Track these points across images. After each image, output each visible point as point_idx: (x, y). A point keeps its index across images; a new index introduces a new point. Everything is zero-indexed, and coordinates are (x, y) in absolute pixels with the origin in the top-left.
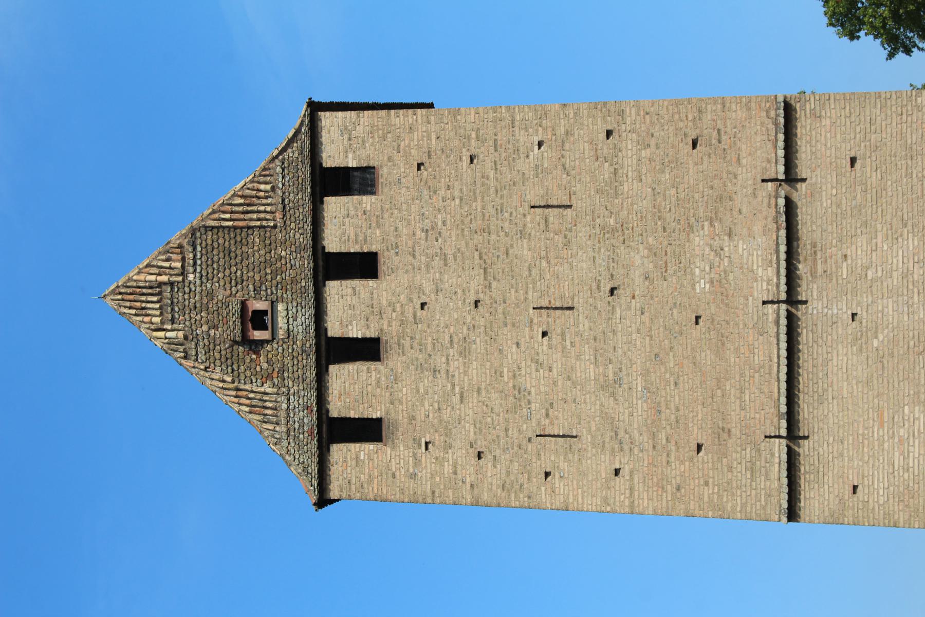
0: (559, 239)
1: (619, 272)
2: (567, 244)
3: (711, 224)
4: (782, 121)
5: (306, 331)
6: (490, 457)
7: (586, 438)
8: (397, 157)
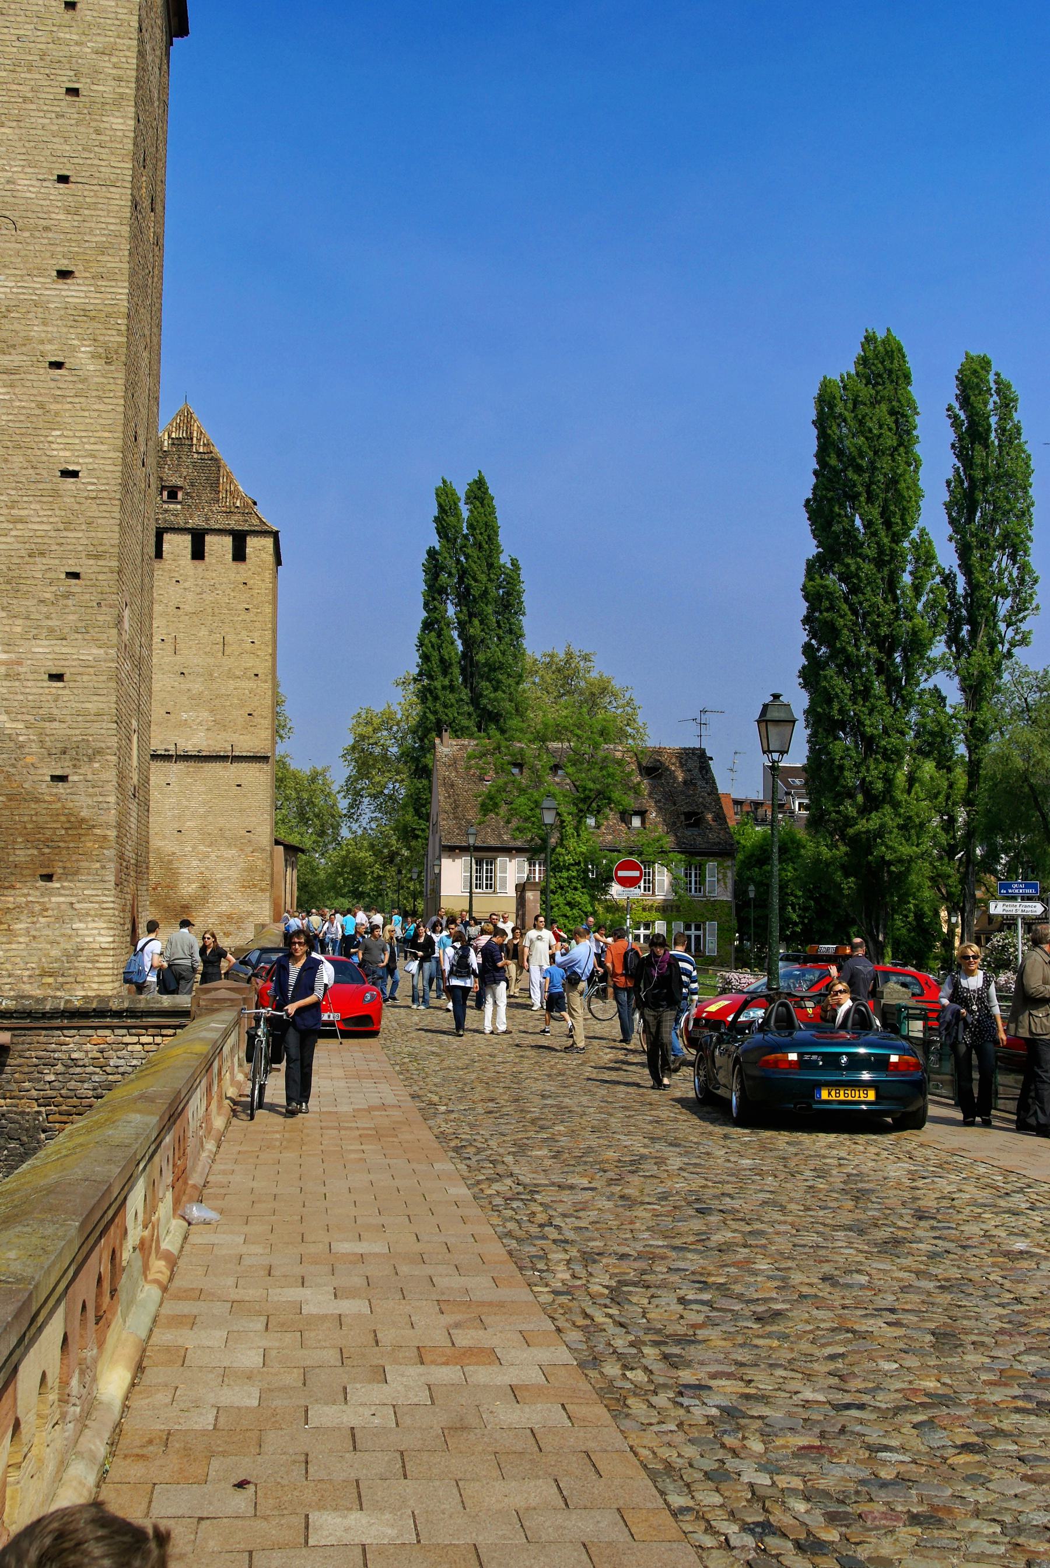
0: (208, 649)
1: (191, 678)
8: (250, 573)
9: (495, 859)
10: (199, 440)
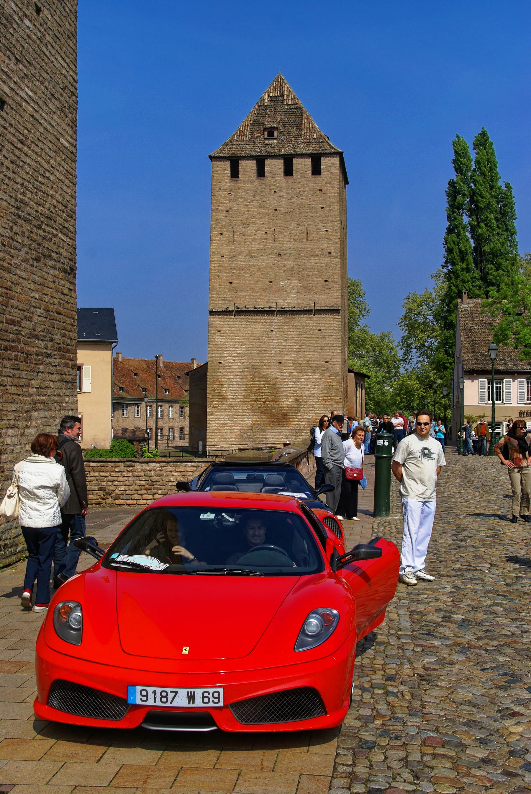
0: (297, 237)
2: (295, 240)
3: (301, 286)
4: (332, 308)
5: (266, 151)
6: (227, 215)
7: (233, 247)
8: (324, 183)
9: (502, 380)
10: (288, 96)
